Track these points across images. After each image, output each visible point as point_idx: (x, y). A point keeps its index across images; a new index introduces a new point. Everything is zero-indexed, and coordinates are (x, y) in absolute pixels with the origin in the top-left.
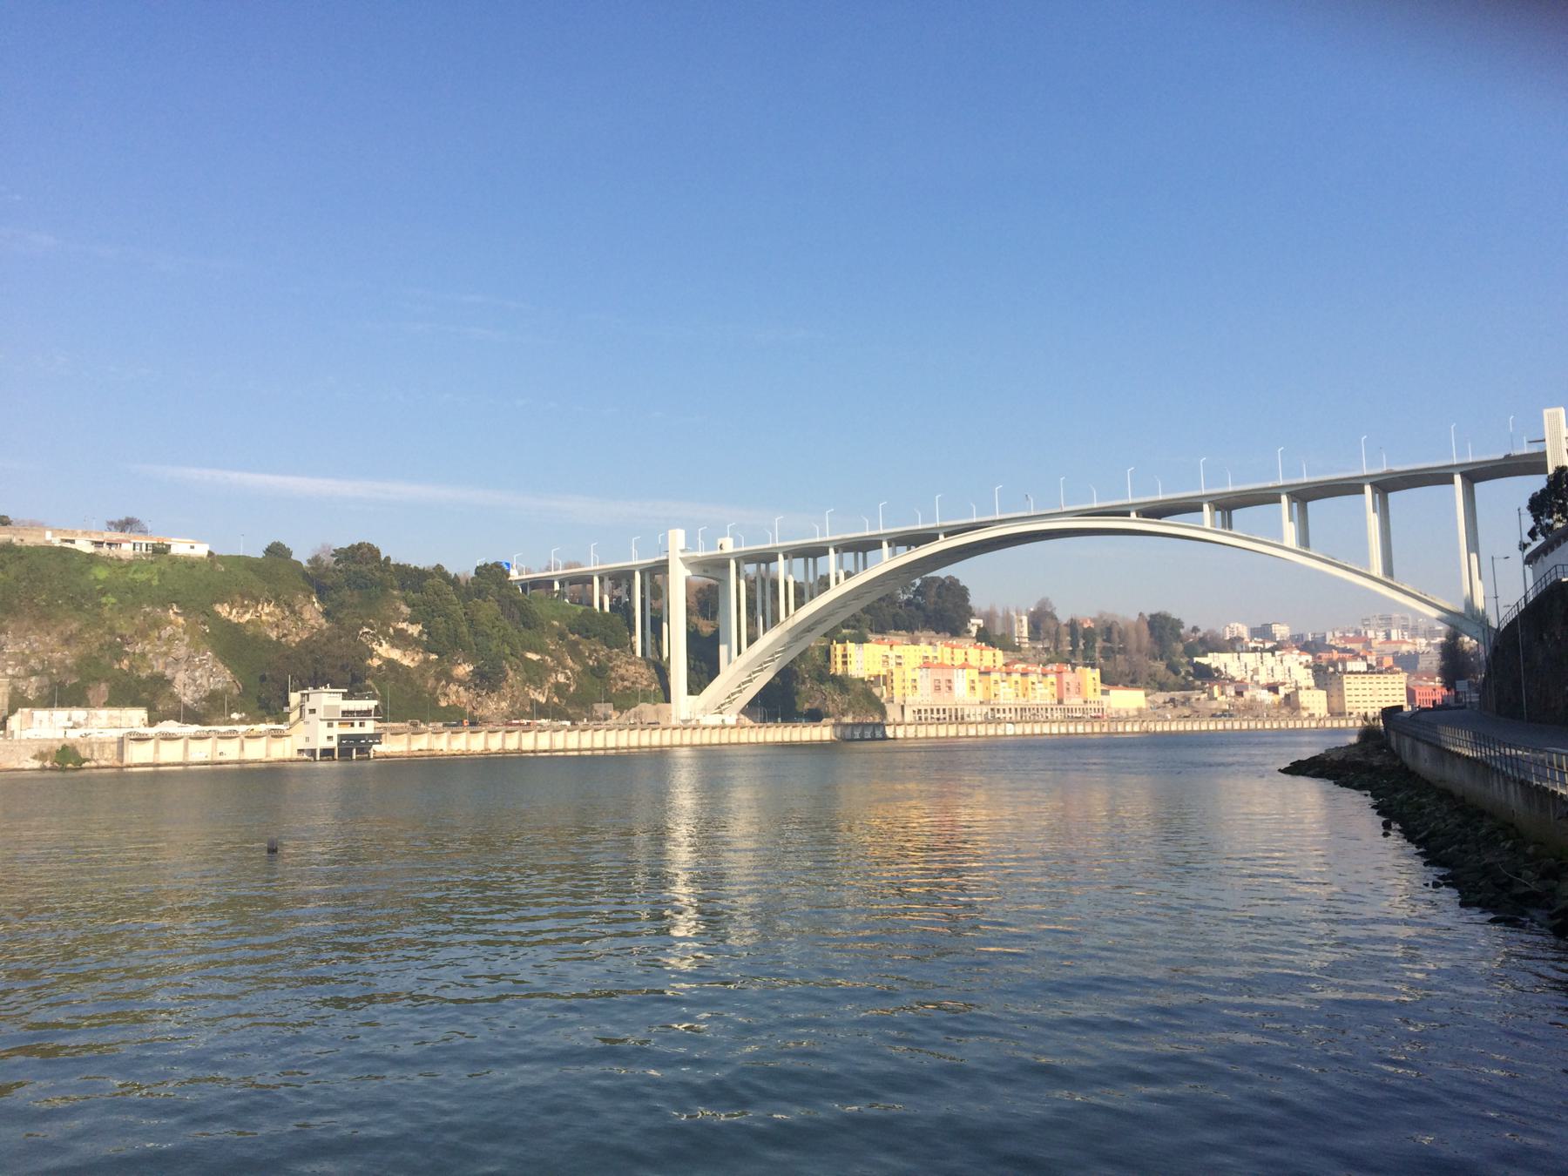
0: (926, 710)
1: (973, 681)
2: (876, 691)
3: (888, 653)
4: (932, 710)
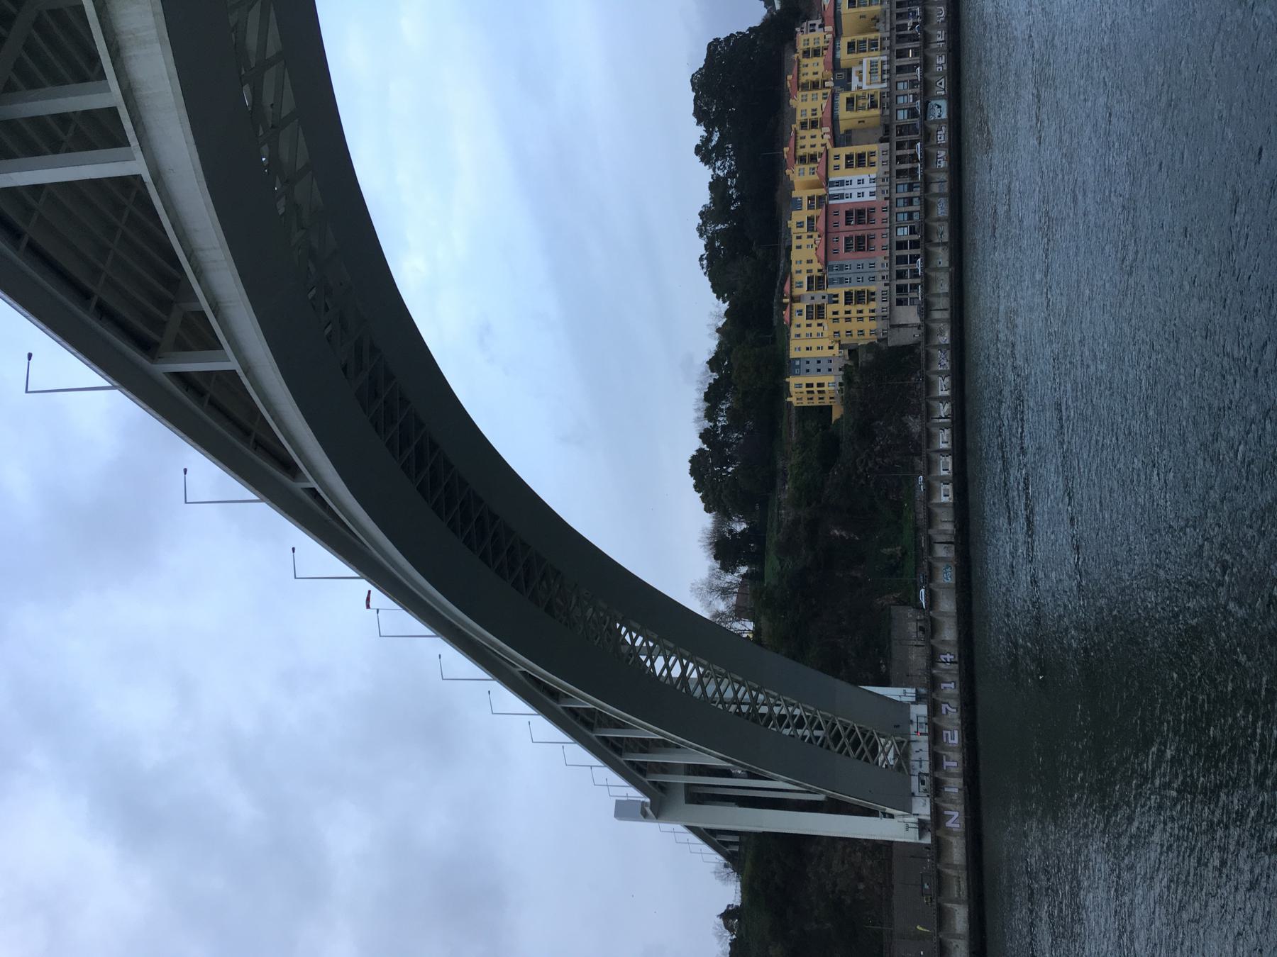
0: (901, 275)
1: (849, 157)
2: (864, 358)
3: (802, 306)
4: (901, 260)
